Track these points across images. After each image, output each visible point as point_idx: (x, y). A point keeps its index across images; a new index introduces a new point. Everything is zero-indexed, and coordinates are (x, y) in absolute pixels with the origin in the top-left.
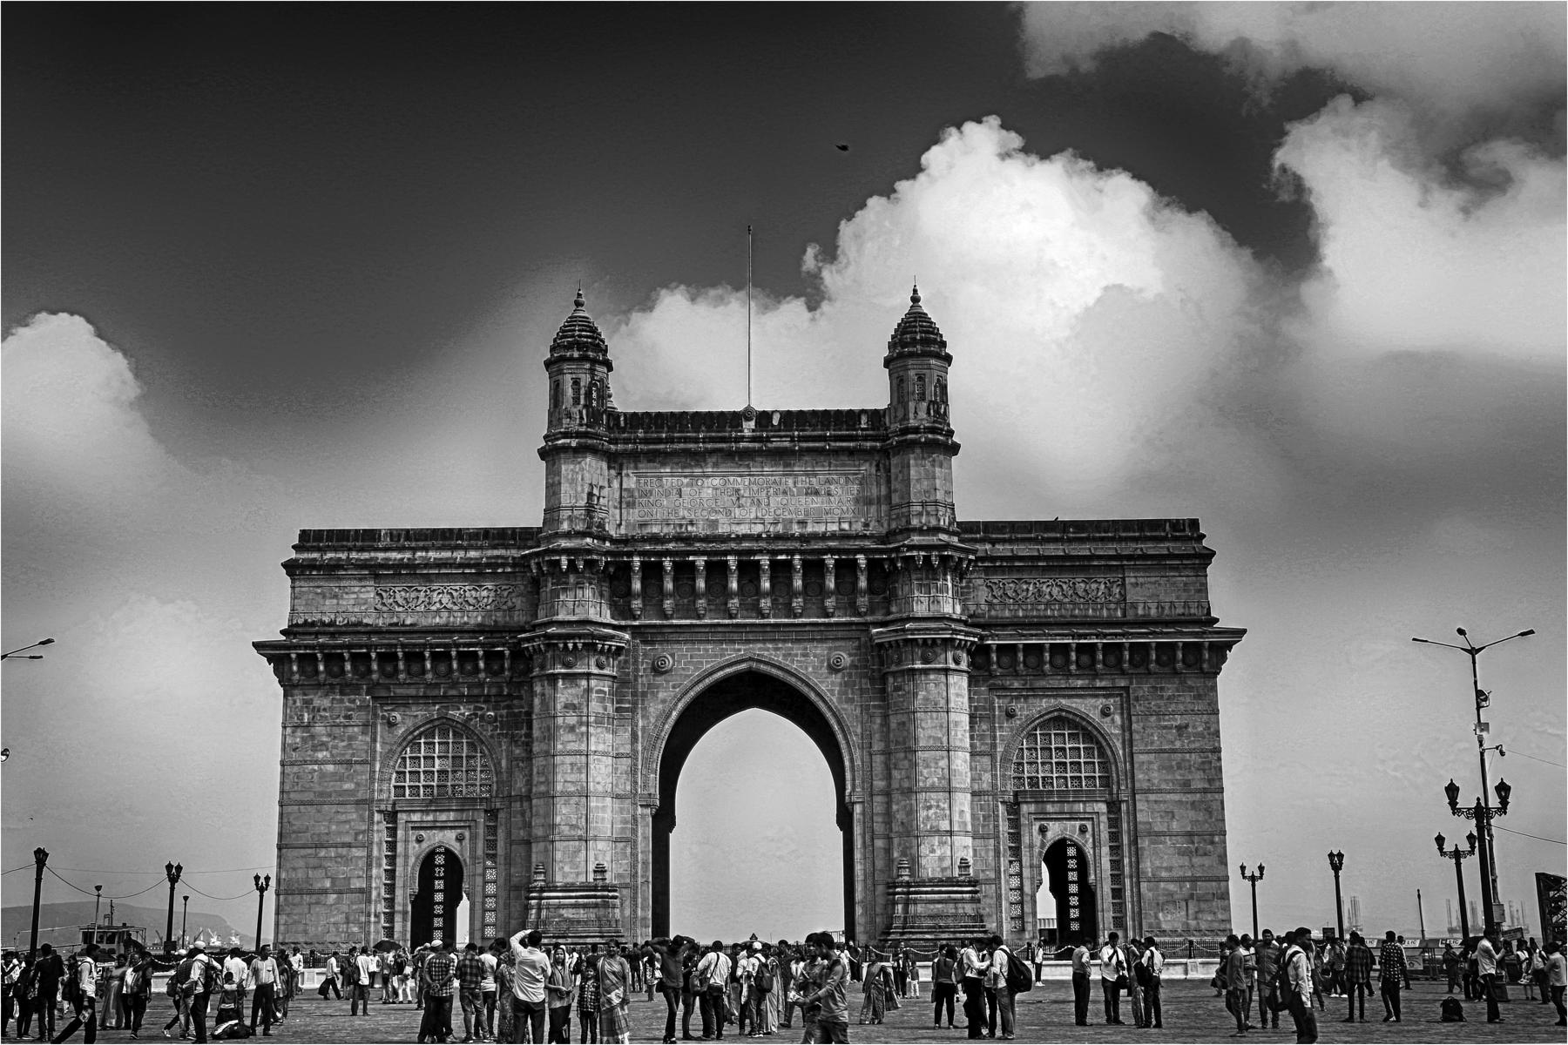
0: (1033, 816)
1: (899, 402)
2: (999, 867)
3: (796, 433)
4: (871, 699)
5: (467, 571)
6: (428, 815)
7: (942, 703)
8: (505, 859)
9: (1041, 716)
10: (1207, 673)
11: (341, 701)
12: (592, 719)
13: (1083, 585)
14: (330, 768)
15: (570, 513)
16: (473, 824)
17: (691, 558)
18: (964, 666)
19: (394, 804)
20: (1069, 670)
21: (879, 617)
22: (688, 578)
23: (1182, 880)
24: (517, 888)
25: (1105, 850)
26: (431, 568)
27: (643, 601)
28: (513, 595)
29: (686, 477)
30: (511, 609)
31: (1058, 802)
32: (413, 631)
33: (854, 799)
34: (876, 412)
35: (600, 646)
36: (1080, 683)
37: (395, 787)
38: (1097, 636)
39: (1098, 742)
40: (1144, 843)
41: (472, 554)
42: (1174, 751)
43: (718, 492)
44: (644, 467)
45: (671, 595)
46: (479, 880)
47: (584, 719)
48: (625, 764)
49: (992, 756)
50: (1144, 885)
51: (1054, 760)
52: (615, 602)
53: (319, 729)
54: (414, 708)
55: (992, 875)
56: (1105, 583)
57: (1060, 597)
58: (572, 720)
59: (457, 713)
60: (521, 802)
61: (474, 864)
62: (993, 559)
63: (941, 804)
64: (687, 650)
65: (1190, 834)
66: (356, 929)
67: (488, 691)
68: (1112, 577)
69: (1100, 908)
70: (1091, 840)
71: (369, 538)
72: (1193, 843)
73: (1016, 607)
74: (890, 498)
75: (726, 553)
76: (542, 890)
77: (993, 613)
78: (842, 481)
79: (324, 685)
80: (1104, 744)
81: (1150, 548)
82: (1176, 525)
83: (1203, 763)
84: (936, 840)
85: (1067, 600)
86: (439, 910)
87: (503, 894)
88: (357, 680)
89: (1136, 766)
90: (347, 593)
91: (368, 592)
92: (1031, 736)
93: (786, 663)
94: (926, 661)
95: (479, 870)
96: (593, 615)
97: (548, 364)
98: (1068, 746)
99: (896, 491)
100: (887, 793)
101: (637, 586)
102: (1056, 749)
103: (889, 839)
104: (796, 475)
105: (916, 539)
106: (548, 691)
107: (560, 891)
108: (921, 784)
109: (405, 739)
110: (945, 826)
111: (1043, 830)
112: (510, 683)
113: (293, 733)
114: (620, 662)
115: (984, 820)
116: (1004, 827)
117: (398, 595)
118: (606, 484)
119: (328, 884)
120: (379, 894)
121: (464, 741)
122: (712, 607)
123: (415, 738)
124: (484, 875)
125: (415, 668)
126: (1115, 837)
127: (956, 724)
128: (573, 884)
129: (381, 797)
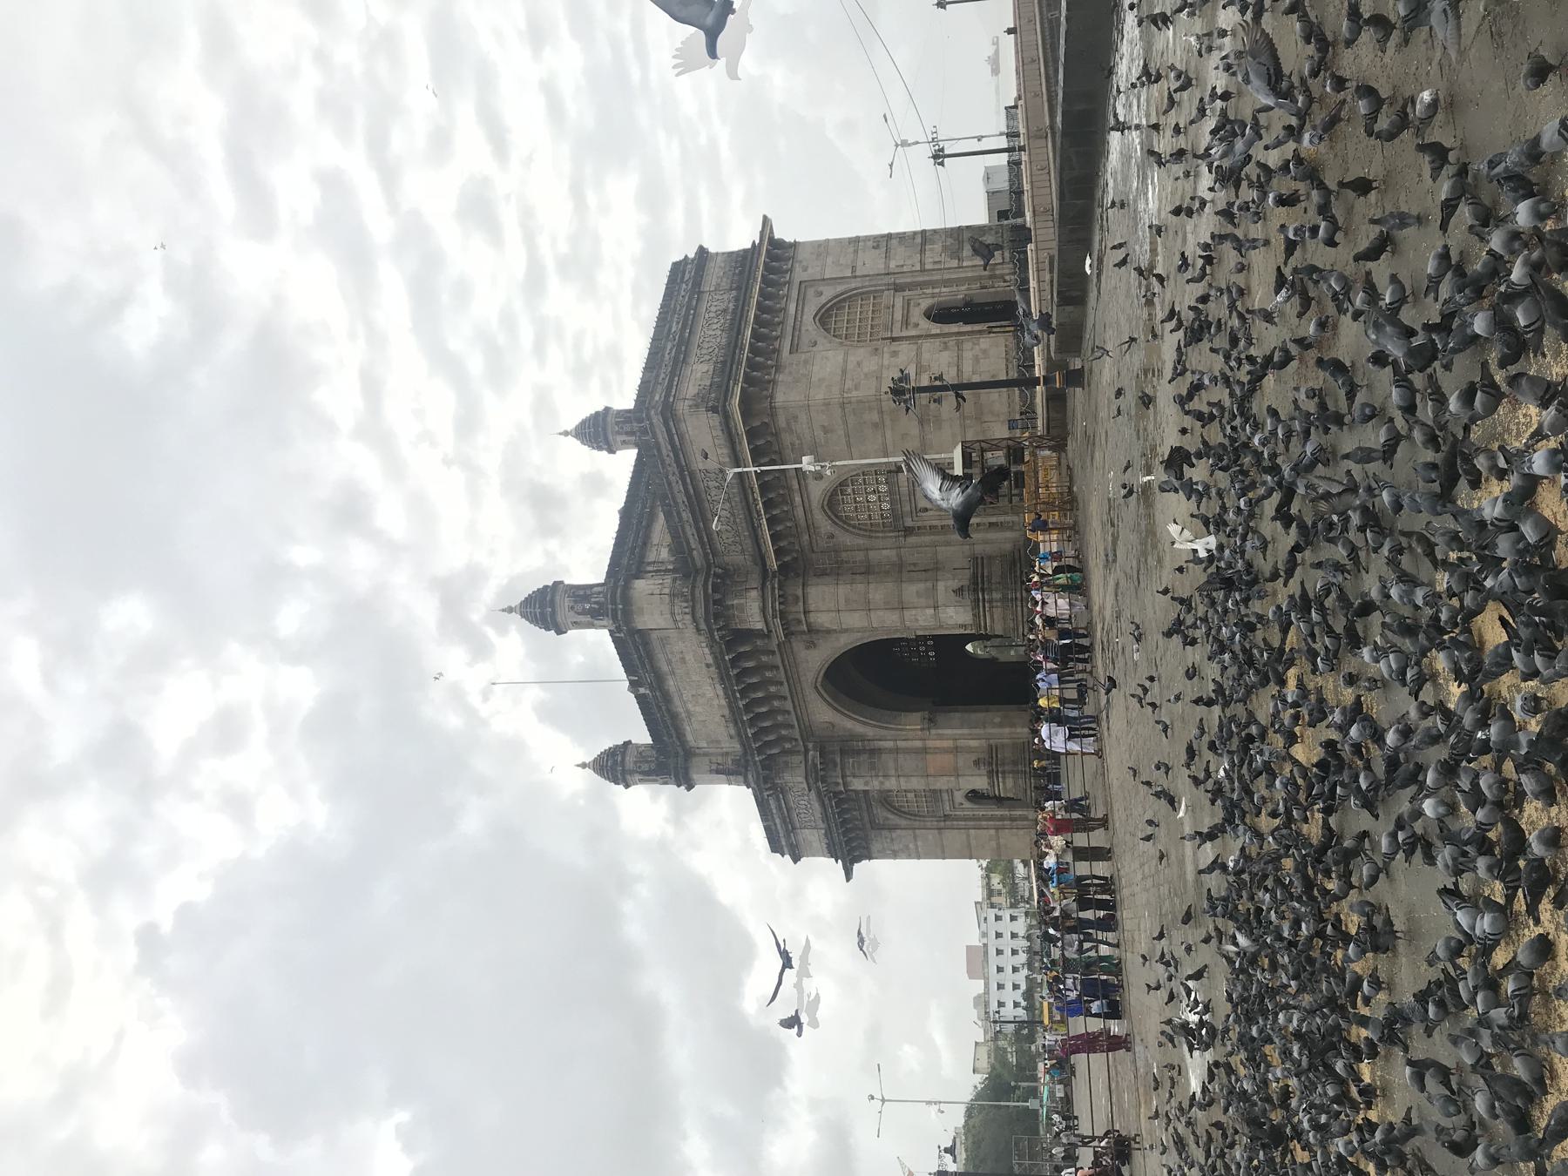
0: (915, 519)
7: (834, 614)
9: (829, 517)
35: (822, 773)
36: (798, 499)
38: (756, 505)
42: (847, 435)
44: (689, 737)
62: (706, 555)
66: (1021, 832)
68: (699, 476)
83: (855, 414)
110: (931, 611)
111: (926, 510)
116: (927, 539)
118: (707, 759)
119: (993, 844)
127: (847, 601)
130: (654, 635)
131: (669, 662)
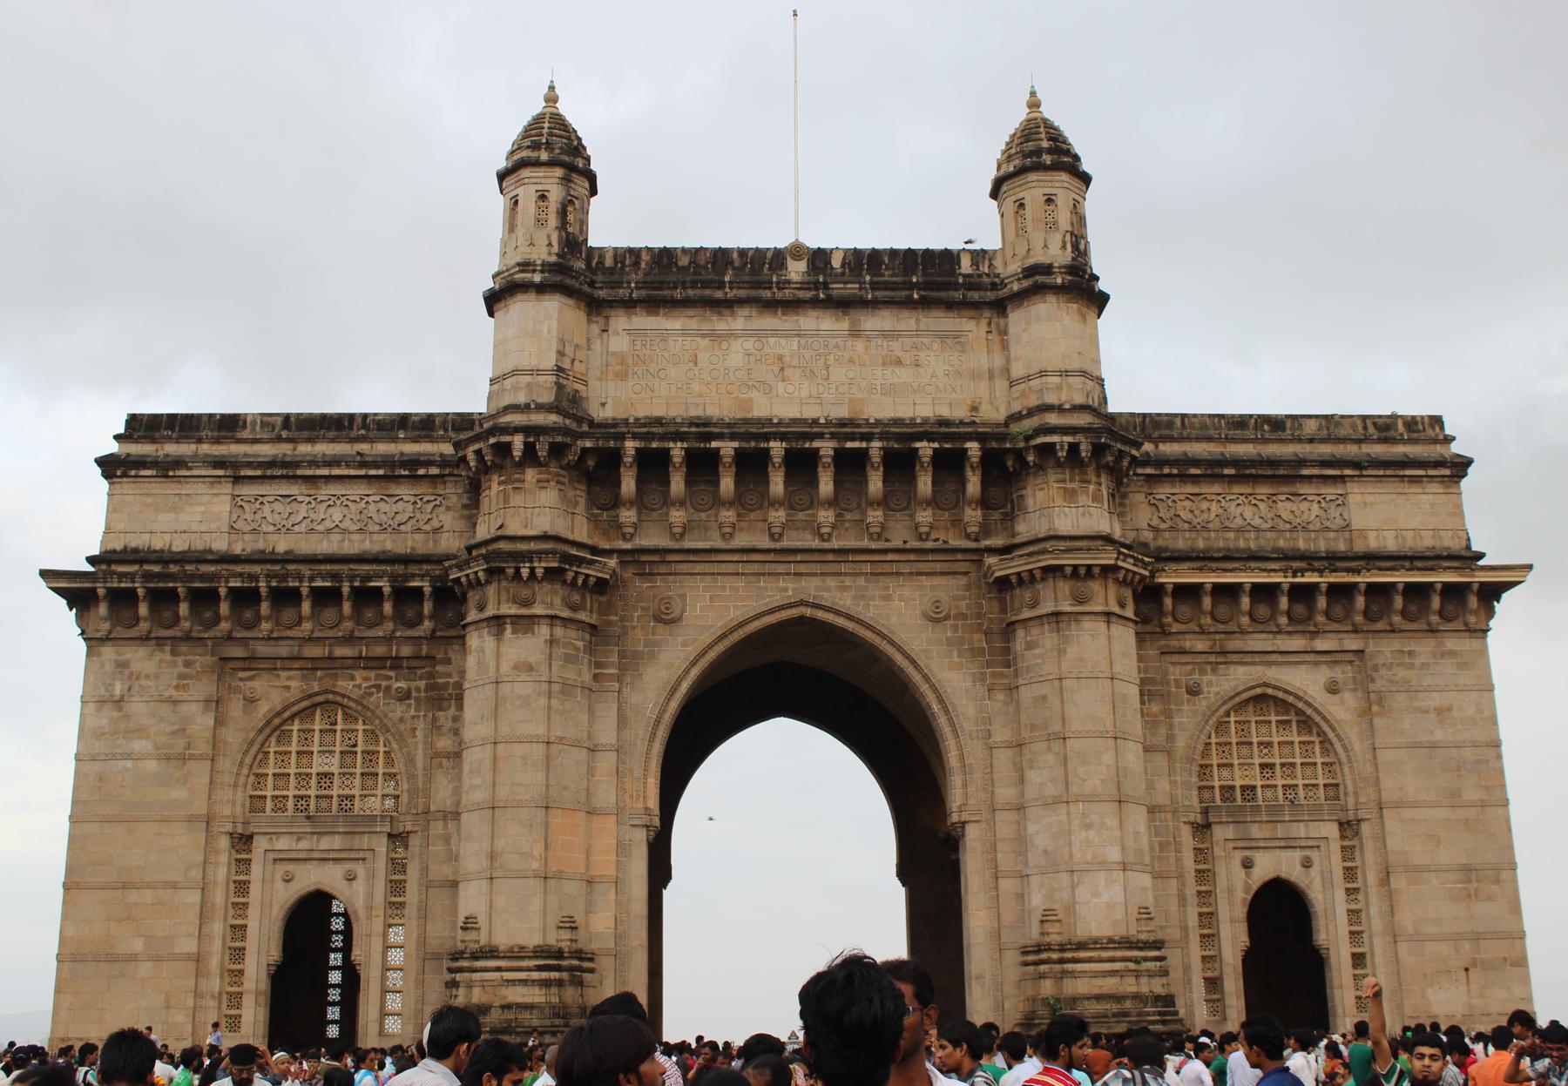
0: (1231, 845)
1: (1017, 235)
2: (1185, 921)
3: (868, 278)
4: (989, 664)
5: (373, 472)
6: (299, 839)
7: (1104, 666)
8: (419, 910)
9: (1238, 694)
10: (1475, 631)
11: (174, 664)
12: (556, 688)
13: (1288, 505)
14: (151, 766)
15: (528, 378)
16: (368, 855)
17: (714, 444)
18: (1129, 612)
19: (246, 823)
20: (1278, 626)
21: (997, 541)
22: (707, 482)
23: (1457, 938)
24: (436, 957)
25: (1340, 895)
26: (318, 467)
27: (639, 513)
28: (442, 509)
29: (703, 336)
30: (436, 531)
31: (1268, 822)
32: (289, 558)
33: (965, 817)
34: (984, 252)
35: (570, 576)
37: (251, 797)
38: (1321, 572)
39: (1323, 732)
40: (1398, 882)
41: (383, 448)
42: (1433, 746)
43: (752, 359)
44: (642, 321)
45: (682, 503)
46: (377, 944)
47: (545, 686)
48: (607, 761)
49: (1169, 753)
50: (1403, 948)
51: (1257, 761)
52: (592, 514)
53: (138, 708)
54: (284, 674)
56: (1319, 502)
57: (1257, 522)
58: (524, 687)
59: (352, 683)
60: (445, 819)
62: (1160, 462)
63: (1108, 821)
64: (706, 589)
65: (1467, 869)
67: (397, 651)
68: (1330, 491)
70: (1318, 880)
71: (229, 425)
72: (1469, 881)
73: (1194, 535)
74: (1008, 370)
75: (767, 437)
76: (475, 956)
77: (1161, 542)
78: (936, 346)
79: (148, 638)
80: (1331, 735)
81: (1378, 450)
82: (1412, 423)
83: (1478, 762)
84: (1101, 877)
85: (1266, 526)
86: (334, 995)
87: (414, 966)
88: (199, 631)
90: (191, 505)
91: (223, 502)
92: (1221, 726)
93: (857, 610)
94: (1080, 601)
95: (378, 925)
96: (561, 528)
97: (502, 176)
98: (1276, 739)
99: (1017, 359)
100: (1021, 808)
101: (628, 485)
102: (1260, 744)
103: (1024, 877)
104: (867, 336)
105: (1053, 419)
107: (504, 957)
108: (1074, 789)
109: (268, 723)
110: (1114, 854)
111: (1248, 864)
112: (432, 637)
113: (97, 711)
114: (600, 604)
115: (1161, 851)
117: (267, 509)
118: (583, 343)
119: (138, 945)
120: (222, 962)
121: (360, 727)
122: (744, 525)
123: (285, 722)
124: (385, 935)
125: (288, 615)
126: (1350, 874)
128: (522, 948)
129: (227, 811)
130: (973, 328)
131: (885, 335)
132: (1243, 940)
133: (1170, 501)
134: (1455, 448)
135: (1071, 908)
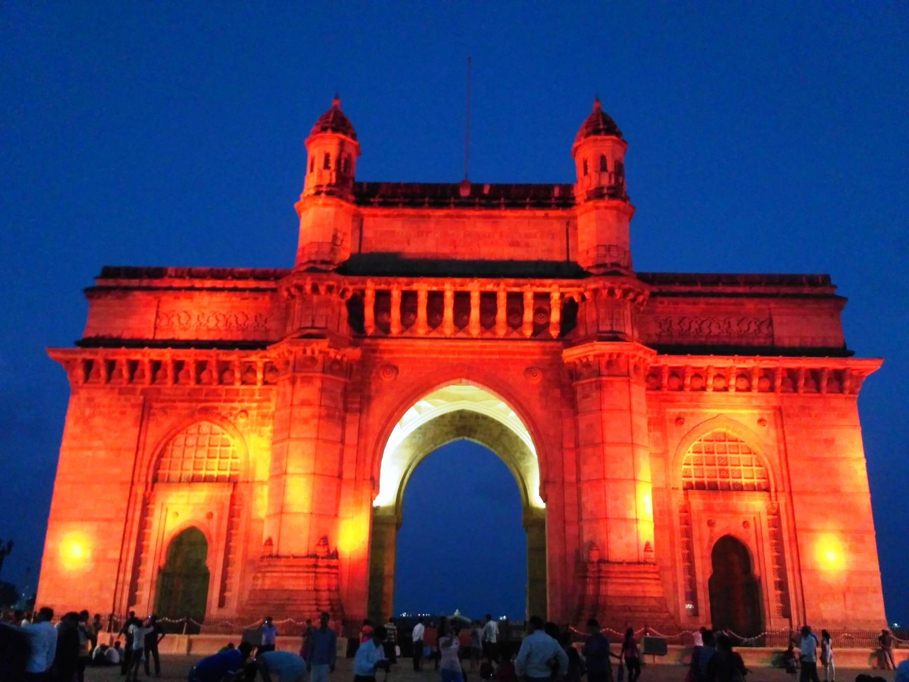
11: (119, 400)
14: (102, 454)
30: (267, 331)
53: (97, 421)
55: (668, 563)
56: (755, 323)
58: (306, 412)
61: (218, 541)
69: (765, 597)
71: (159, 273)
78: (538, 235)
89: (791, 472)
95: (222, 544)
106: (289, 388)
108: (608, 476)
109: (169, 433)
111: (711, 524)
118: (350, 232)
132: (709, 570)
133: (668, 322)
134: (838, 292)
135: (605, 546)
